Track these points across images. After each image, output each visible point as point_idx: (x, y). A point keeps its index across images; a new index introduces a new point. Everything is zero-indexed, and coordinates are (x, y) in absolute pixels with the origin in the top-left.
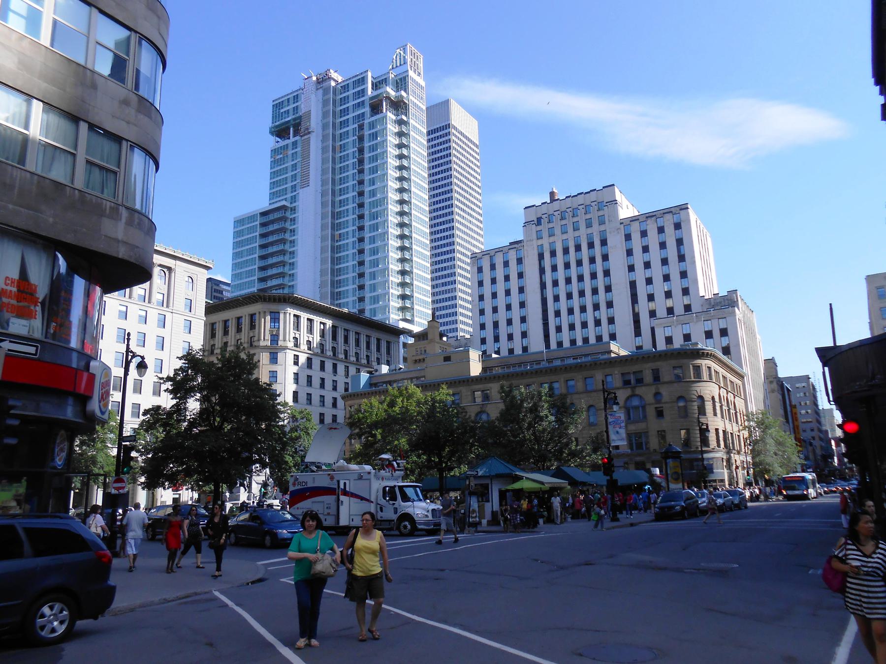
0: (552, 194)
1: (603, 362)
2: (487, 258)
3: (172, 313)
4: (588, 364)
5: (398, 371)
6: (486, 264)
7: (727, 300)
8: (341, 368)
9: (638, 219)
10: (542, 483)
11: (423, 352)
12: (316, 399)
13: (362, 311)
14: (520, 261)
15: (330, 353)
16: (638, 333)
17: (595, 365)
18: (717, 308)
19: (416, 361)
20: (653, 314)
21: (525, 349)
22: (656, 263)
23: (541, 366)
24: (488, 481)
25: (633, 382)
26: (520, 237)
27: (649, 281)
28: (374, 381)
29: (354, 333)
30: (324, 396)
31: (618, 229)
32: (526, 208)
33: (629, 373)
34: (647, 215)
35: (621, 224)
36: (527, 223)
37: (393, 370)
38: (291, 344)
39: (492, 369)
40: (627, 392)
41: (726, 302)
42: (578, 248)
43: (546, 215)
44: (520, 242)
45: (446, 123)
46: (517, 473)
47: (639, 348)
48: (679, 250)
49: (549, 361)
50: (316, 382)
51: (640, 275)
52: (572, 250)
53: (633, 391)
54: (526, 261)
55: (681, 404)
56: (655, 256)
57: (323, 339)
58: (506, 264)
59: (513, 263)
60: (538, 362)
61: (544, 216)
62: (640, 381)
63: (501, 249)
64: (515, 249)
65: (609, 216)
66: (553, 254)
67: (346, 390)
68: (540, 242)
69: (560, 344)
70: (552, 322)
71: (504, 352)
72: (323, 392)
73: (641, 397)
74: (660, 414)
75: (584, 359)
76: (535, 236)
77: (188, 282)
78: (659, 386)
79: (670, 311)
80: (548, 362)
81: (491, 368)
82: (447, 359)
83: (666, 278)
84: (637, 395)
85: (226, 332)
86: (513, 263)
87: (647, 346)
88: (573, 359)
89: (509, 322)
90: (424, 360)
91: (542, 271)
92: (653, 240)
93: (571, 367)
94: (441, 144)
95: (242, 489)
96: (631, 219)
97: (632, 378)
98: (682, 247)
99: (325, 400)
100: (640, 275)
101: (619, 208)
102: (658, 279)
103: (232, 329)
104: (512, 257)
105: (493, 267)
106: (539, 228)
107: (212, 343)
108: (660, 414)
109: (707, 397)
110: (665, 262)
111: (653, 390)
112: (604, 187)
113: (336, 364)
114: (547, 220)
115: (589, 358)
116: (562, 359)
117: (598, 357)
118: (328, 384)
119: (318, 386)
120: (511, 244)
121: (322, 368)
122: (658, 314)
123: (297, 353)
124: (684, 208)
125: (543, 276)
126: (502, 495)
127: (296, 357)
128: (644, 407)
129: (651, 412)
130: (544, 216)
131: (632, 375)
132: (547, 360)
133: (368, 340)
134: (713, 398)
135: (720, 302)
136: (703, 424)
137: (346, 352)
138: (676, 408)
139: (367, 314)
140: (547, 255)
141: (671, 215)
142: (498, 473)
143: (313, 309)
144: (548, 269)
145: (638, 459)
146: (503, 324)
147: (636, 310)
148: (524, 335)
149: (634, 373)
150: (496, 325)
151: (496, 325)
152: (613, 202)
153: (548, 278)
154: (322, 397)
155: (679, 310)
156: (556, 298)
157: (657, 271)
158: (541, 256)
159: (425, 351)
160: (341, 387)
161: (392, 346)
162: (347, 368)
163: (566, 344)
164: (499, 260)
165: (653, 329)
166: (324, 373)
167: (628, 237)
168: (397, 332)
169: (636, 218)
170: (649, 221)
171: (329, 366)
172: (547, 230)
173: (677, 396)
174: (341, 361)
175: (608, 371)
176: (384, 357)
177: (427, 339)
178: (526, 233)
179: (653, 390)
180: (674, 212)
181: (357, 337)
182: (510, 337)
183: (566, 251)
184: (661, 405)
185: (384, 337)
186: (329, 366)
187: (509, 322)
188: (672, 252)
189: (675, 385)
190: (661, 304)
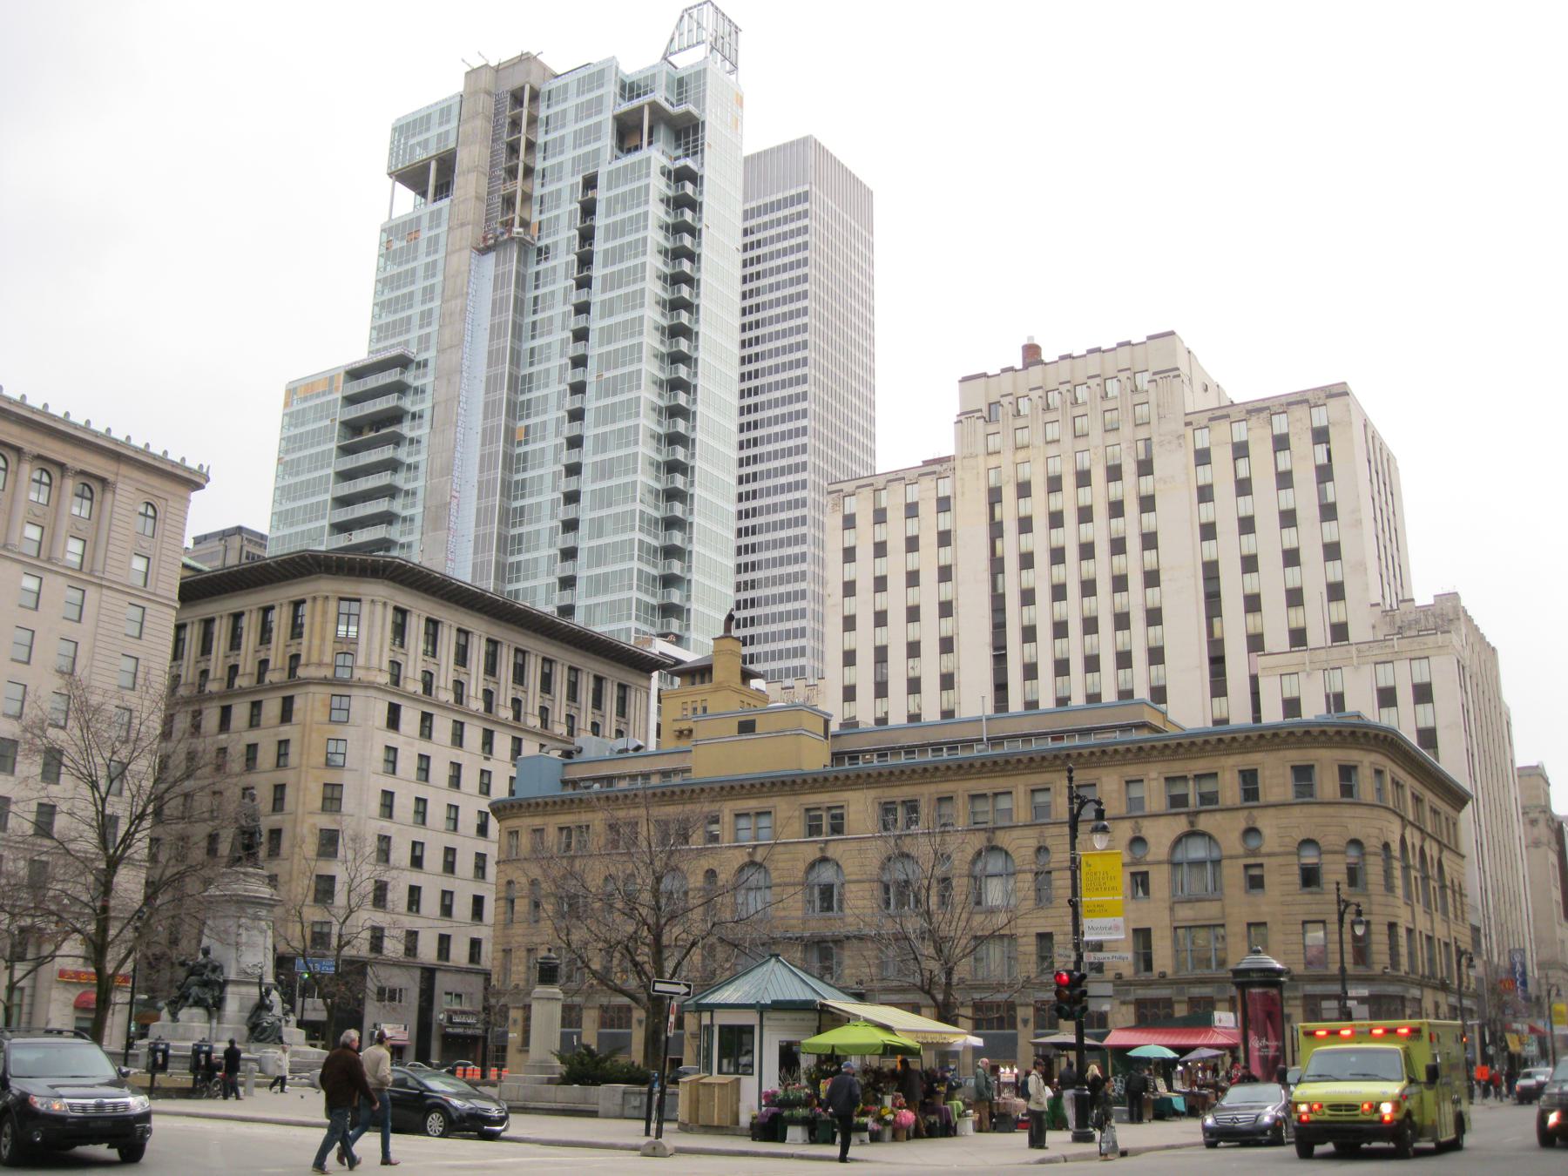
0: (1032, 353)
1: (1120, 748)
2: (868, 492)
3: (101, 586)
4: (1086, 752)
5: (631, 753)
6: (861, 507)
7: (1433, 615)
8: (503, 743)
9: (1228, 416)
10: (887, 1028)
11: (700, 711)
12: (437, 813)
13: (568, 610)
14: (944, 504)
15: (477, 705)
16: (1219, 687)
17: (1104, 757)
18: (1408, 634)
19: (681, 732)
20: (1256, 643)
21: (948, 714)
22: (1267, 522)
23: (975, 753)
24: (750, 1018)
25: (1193, 800)
26: (948, 449)
27: (1250, 564)
28: (576, 773)
29: (540, 661)
30: (457, 808)
31: (1179, 437)
32: (965, 380)
33: (1184, 778)
34: (1249, 407)
35: (1188, 424)
36: (966, 415)
37: (621, 751)
38: (385, 679)
39: (857, 758)
40: (1181, 825)
41: (1431, 620)
42: (1083, 479)
43: (1010, 399)
44: (947, 459)
45: (801, 190)
46: (829, 1002)
47: (1216, 722)
48: (1322, 494)
49: (996, 741)
50: (440, 771)
51: (1228, 548)
52: (1069, 482)
53: (1192, 824)
54: (958, 505)
55: (1310, 858)
56: (1265, 503)
57: (463, 670)
58: (912, 510)
59: (928, 509)
60: (968, 744)
61: (1005, 401)
62: (1209, 799)
63: (901, 475)
64: (935, 476)
65: (1158, 406)
66: (1024, 490)
67: (512, 792)
68: (993, 461)
69: (1031, 705)
70: (1015, 657)
71: (898, 718)
72: (454, 798)
73: (1210, 837)
74: (1256, 883)
75: (1077, 741)
76: (981, 449)
77: (145, 515)
78: (1255, 812)
79: (1298, 637)
80: (993, 745)
81: (853, 756)
82: (747, 727)
83: (1291, 558)
84: (1202, 834)
85: (235, 642)
86: (928, 509)
87: (1240, 716)
88: (1054, 739)
89: (914, 649)
90: (691, 731)
91: (996, 530)
92: (1261, 465)
93: (1043, 758)
94: (784, 236)
95: (199, 1012)
96: (1209, 414)
97: (1192, 791)
98: (1329, 485)
99: (460, 817)
100: (1228, 548)
101: (1187, 390)
102: (1271, 561)
103: (250, 637)
104: (925, 494)
105: (880, 516)
106: (992, 428)
107: (203, 666)
108: (1256, 883)
109: (1372, 844)
110: (1288, 518)
111: (1240, 821)
112: (1150, 338)
113: (491, 732)
114: (1010, 410)
115: (1093, 740)
116: (1026, 737)
117: (1113, 735)
118: (470, 779)
119: (445, 782)
120: (927, 463)
121: (458, 739)
122: (1268, 647)
123: (396, 700)
124: (1338, 392)
125: (998, 543)
126: (789, 1058)
127: (394, 711)
128: (1217, 863)
129: (1233, 874)
130: (1005, 401)
131: (1191, 783)
132: (988, 739)
133: (573, 679)
134: (1386, 846)
135: (1417, 622)
136: (1347, 904)
137: (459, 686)
138: (1296, 870)
139: (579, 620)
140: (1009, 493)
141: (1305, 407)
142: (781, 998)
143: (442, 597)
144: (1010, 527)
145: (1196, 991)
146: (897, 656)
147: (1217, 634)
148: (947, 682)
149: (1198, 777)
150: (881, 654)
151: (881, 654)
152: (1172, 374)
153: (1010, 547)
154: (454, 808)
155: (1318, 635)
156: (1028, 597)
157: (1269, 542)
158: (995, 496)
159: (705, 709)
160: (500, 791)
161: (633, 698)
162: (517, 743)
163: (1047, 702)
164: (893, 501)
165: (1254, 680)
166: (459, 752)
167: (1203, 457)
168: (644, 665)
169: (1224, 412)
170: (1254, 421)
171: (473, 735)
172: (1011, 430)
173: (1300, 839)
174: (503, 724)
175: (1132, 771)
176: (610, 722)
177: (711, 681)
178: (961, 438)
179: (1240, 821)
180: (1312, 402)
181: (547, 671)
182: (914, 686)
183: (1054, 484)
184: (1258, 860)
185: (614, 675)
186: (473, 735)
187: (914, 649)
188: (1304, 497)
189: (1296, 811)
190: (1275, 622)
